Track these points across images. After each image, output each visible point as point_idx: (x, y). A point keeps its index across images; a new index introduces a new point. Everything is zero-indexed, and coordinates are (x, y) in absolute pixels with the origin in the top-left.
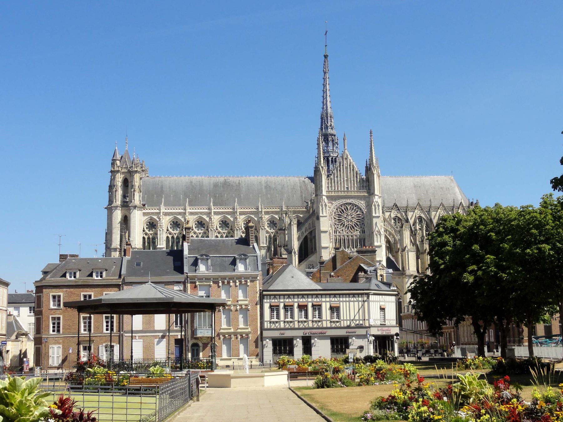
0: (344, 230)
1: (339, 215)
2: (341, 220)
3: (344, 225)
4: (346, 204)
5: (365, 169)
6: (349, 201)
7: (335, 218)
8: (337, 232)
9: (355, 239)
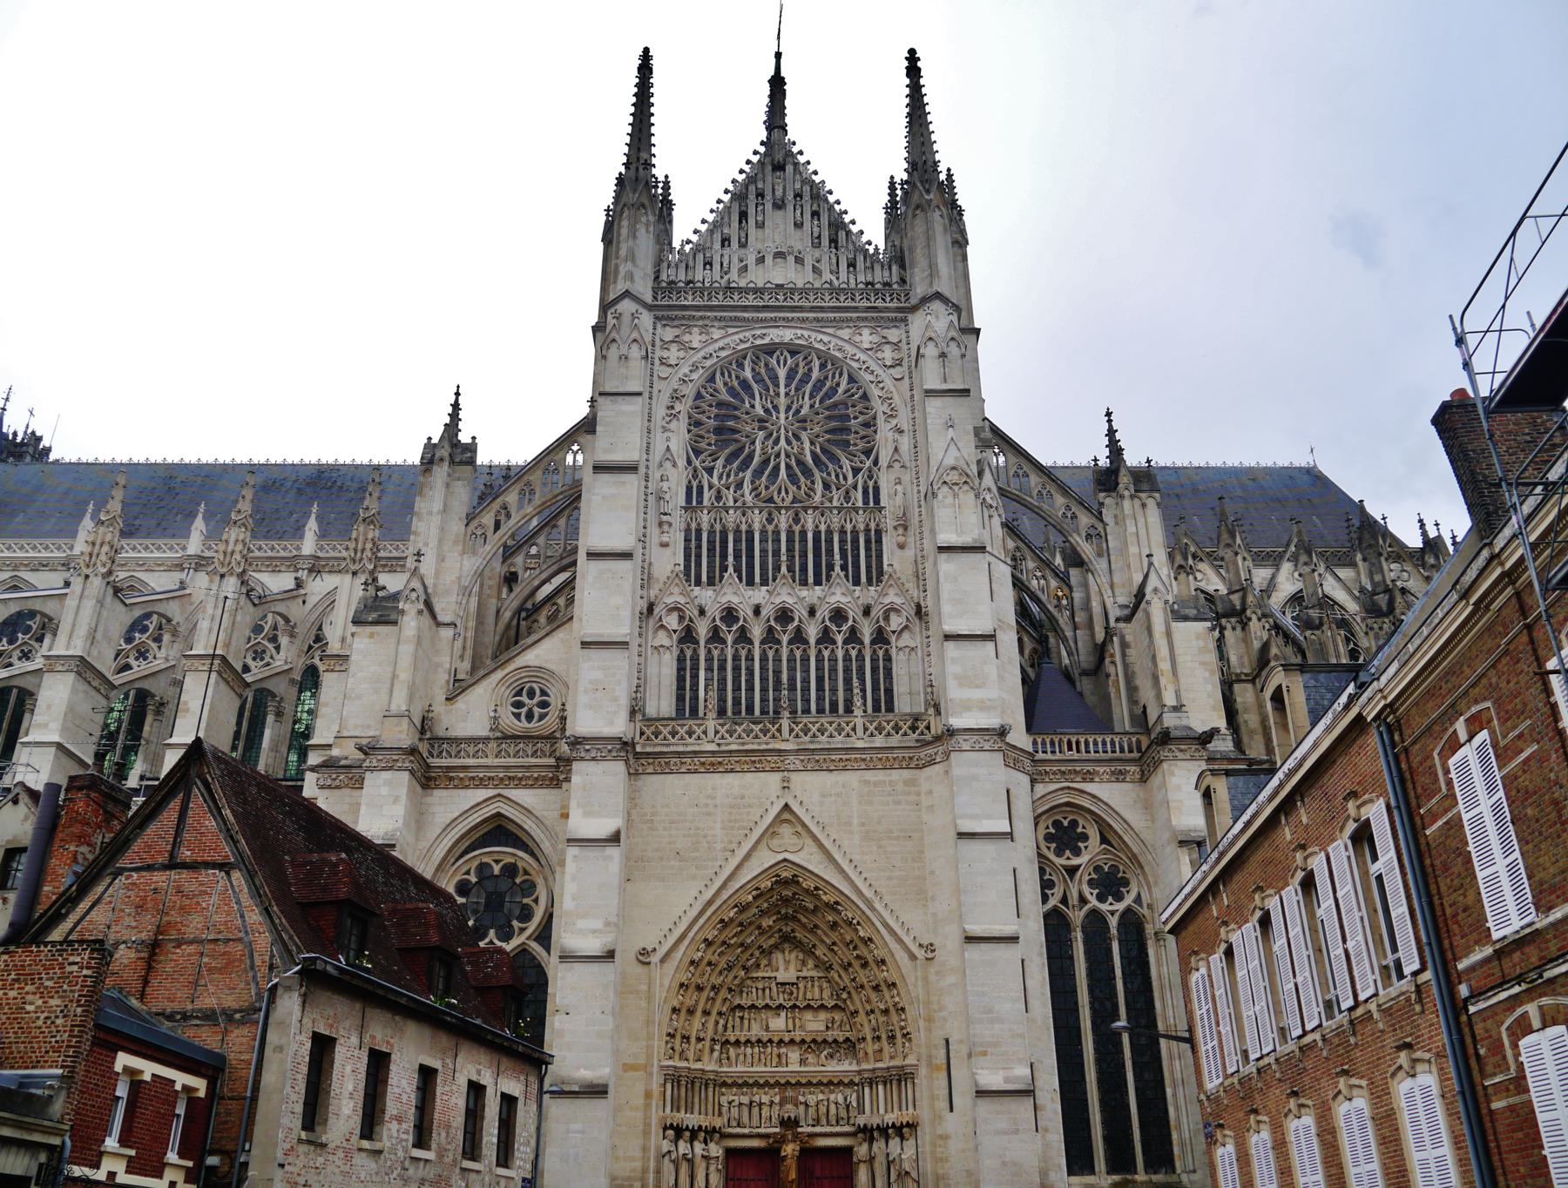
0: (747, 487)
1: (720, 404)
2: (735, 431)
3: (751, 456)
4: (770, 350)
6: (787, 335)
7: (698, 424)
9: (817, 534)
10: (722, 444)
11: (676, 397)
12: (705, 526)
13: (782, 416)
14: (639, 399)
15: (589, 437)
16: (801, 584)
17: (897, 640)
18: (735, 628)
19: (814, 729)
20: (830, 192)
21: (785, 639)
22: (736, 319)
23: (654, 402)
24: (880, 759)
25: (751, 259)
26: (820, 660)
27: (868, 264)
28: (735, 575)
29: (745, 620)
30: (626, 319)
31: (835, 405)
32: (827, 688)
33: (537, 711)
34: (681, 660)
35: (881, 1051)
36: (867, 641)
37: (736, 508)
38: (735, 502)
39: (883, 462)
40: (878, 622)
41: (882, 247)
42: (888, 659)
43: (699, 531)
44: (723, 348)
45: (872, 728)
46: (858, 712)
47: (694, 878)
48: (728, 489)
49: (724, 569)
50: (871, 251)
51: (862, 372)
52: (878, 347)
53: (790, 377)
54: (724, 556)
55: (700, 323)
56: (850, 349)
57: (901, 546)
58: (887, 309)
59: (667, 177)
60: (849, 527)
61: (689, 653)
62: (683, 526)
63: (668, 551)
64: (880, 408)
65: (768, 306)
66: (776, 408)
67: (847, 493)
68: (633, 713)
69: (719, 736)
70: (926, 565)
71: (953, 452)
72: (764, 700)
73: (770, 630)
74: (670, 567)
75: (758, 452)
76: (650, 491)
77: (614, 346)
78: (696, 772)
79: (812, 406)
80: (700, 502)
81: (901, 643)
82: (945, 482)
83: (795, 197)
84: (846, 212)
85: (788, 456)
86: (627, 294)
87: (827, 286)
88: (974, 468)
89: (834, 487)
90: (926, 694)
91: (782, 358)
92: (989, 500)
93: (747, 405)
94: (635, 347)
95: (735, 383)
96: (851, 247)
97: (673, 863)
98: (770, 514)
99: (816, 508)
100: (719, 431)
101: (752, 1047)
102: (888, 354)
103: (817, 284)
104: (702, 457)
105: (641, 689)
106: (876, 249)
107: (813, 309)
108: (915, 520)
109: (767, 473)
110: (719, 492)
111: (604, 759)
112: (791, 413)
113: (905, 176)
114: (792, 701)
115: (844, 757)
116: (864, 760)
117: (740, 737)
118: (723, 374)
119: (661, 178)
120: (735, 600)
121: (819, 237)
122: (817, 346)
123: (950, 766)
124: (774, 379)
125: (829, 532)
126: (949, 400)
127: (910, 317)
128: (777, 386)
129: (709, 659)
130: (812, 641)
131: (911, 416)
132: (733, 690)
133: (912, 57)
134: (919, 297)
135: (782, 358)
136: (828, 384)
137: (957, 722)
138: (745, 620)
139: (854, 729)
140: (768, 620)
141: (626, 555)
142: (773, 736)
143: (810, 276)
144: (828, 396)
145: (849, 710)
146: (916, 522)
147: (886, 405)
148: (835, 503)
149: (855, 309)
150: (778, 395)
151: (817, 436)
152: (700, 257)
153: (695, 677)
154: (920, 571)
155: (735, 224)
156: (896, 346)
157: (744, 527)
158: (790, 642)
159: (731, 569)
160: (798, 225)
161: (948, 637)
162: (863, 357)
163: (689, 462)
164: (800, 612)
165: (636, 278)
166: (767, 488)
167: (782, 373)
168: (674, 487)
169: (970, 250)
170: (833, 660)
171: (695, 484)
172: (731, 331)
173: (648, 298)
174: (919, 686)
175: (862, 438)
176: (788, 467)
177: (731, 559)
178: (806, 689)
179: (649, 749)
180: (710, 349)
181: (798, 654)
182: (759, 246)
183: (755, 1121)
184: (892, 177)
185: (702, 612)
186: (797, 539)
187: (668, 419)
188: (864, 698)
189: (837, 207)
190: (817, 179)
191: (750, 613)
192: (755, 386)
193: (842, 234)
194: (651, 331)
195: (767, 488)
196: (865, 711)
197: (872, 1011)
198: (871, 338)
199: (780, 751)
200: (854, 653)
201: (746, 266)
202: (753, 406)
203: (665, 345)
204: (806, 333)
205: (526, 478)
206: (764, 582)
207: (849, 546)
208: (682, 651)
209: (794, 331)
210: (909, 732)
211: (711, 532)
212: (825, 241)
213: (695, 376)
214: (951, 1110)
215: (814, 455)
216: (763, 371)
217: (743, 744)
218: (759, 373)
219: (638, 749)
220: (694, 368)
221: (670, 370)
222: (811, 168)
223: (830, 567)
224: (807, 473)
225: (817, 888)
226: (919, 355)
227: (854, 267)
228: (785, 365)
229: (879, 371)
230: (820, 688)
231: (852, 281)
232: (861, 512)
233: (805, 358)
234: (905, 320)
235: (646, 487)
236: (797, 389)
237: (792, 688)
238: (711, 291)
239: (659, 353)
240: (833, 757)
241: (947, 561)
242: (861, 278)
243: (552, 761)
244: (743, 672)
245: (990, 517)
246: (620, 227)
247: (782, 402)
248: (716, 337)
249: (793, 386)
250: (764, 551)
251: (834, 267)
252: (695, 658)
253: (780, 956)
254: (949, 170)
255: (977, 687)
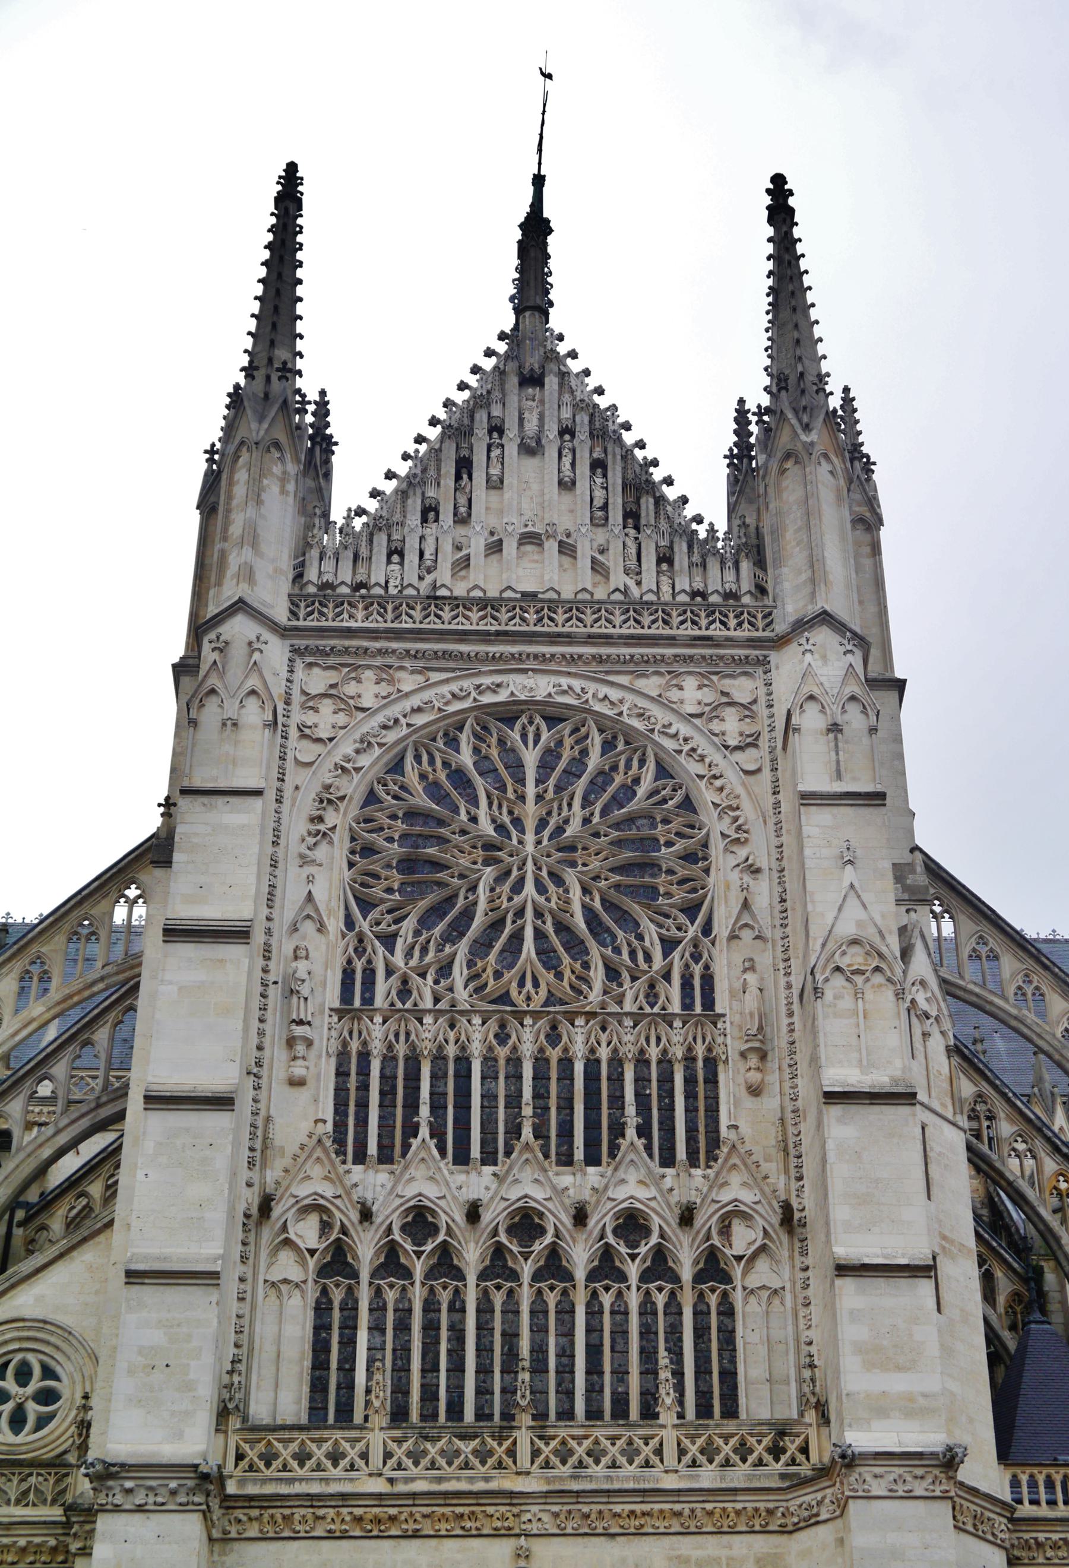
0: (459, 973)
1: (412, 815)
2: (438, 865)
3: (468, 914)
5: (722, 471)
7: (368, 851)
8: (381, 986)
9: (592, 1065)
10: (413, 890)
11: (328, 799)
12: (377, 1048)
13: (530, 838)
14: (257, 803)
15: (159, 873)
16: (559, 1163)
17: (745, 1273)
18: (429, 1247)
19: (580, 1451)
20: (627, 426)
21: (527, 1270)
22: (447, 655)
23: (285, 808)
24: (710, 1514)
25: (477, 546)
26: (594, 1311)
27: (696, 558)
28: (432, 1144)
29: (449, 1232)
30: (238, 652)
31: (631, 820)
32: (607, 1368)
33: (33, 1409)
34: (322, 1308)
36: (687, 1274)
37: (438, 1014)
38: (437, 1000)
39: (721, 928)
40: (708, 1237)
41: (722, 527)
42: (727, 1311)
43: (364, 1057)
44: (419, 710)
45: (693, 1449)
46: (667, 1417)
48: (423, 975)
49: (411, 1130)
50: (702, 534)
51: (682, 759)
52: (711, 713)
53: (545, 766)
54: (412, 1105)
55: (378, 661)
56: (660, 715)
57: (755, 1091)
58: (730, 642)
59: (323, 393)
60: (654, 1053)
61: (337, 1296)
62: (334, 1046)
63: (303, 1095)
64: (714, 824)
65: (506, 633)
66: (517, 822)
67: (652, 986)
68: (223, 1414)
69: (390, 1463)
70: (802, 1127)
71: (853, 911)
72: (483, 1391)
73: (499, 1251)
74: (307, 1126)
75: (482, 906)
76: (272, 977)
77: (213, 700)
78: (344, 1536)
79: (586, 821)
80: (368, 999)
81: (754, 1280)
82: (838, 969)
83: (562, 432)
84: (655, 463)
85: (539, 914)
86: (240, 606)
87: (617, 596)
88: (894, 944)
89: (626, 975)
90: (801, 1381)
91: (531, 730)
92: (922, 1004)
93: (463, 817)
94: (252, 703)
95: (442, 776)
96: (664, 525)
98: (503, 1026)
99: (591, 1015)
100: (407, 865)
102: (732, 725)
103: (600, 594)
104: (374, 914)
105: (242, 1367)
106: (712, 530)
107: (591, 639)
108: (781, 1041)
109: (498, 946)
110: (405, 981)
111: (160, 1508)
112: (546, 833)
113: (765, 401)
114: (539, 1393)
115: (638, 1508)
116: (678, 1514)
117: (433, 1465)
118: (418, 758)
119: (313, 396)
120: (431, 1191)
121: (605, 507)
122: (598, 707)
123: (847, 1529)
124: (517, 768)
125: (616, 1062)
126: (845, 813)
127: (774, 657)
128: (522, 781)
129: (378, 1308)
130: (580, 1274)
131: (775, 842)
132: (423, 1371)
133: (779, 188)
134: (791, 619)
135: (531, 730)
136: (618, 779)
137: (859, 1439)
138: (449, 1232)
139: (659, 1452)
140: (495, 1233)
141: (222, 1102)
142: (500, 1465)
143: (587, 578)
144: (617, 801)
145: (649, 1413)
146: (784, 1044)
147: (727, 820)
148: (629, 1006)
149: (671, 641)
150: (522, 798)
151: (596, 878)
152: (381, 540)
153: (349, 1343)
154: (791, 1140)
155: (449, 482)
156: (748, 710)
157: (451, 1051)
158: (537, 1277)
159: (424, 1132)
160: (566, 485)
161: (843, 1269)
162: (684, 730)
163: (350, 923)
164: (557, 1217)
165: (259, 576)
166: (498, 975)
167: (531, 758)
168: (317, 968)
169: (886, 535)
170: (620, 1312)
171: (359, 965)
172: (435, 676)
173: (281, 614)
174: (788, 1366)
175: (682, 882)
176: (540, 935)
177: (425, 1111)
178: (566, 1370)
179: (252, 1490)
180: (395, 711)
181: (552, 1299)
182: (493, 522)
184: (741, 402)
185: (366, 1215)
186: (554, 1075)
187: (311, 840)
188: (680, 1388)
189: (639, 454)
190: (603, 402)
191: (460, 1217)
192: (479, 782)
193: (647, 504)
194: (284, 674)
195: (498, 975)
196: (681, 1416)
198: (699, 695)
199: (511, 1494)
200: (660, 1299)
201: (468, 558)
202: (474, 819)
203: (310, 703)
204: (577, 684)
205: (34, 949)
206: (489, 1157)
207: (654, 1089)
208: (325, 1291)
209: (554, 679)
210: (768, 1458)
211: (389, 1059)
212: (616, 515)
213: (364, 761)
215: (591, 917)
216: (494, 752)
217: (439, 1480)
218: (487, 757)
219: (231, 1488)
220: (365, 745)
221: (318, 748)
222: (592, 382)
223: (618, 1130)
224: (576, 946)
226: (788, 726)
227: (670, 561)
228: (536, 742)
229: (715, 756)
230: (594, 1368)
231: (666, 588)
232: (677, 1024)
233: (576, 730)
234: (763, 662)
235: (265, 971)
236: (559, 789)
237: (539, 1367)
238: (400, 604)
239: (298, 716)
240: (617, 1509)
241: (840, 1120)
242: (683, 583)
243: (56, 1513)
244: (444, 1334)
245: (926, 1035)
246: (231, 483)
247: (531, 811)
248: (406, 688)
249: (552, 782)
250: (488, 1098)
251: (632, 563)
252: (350, 1307)
254: (846, 390)
255: (899, 1368)
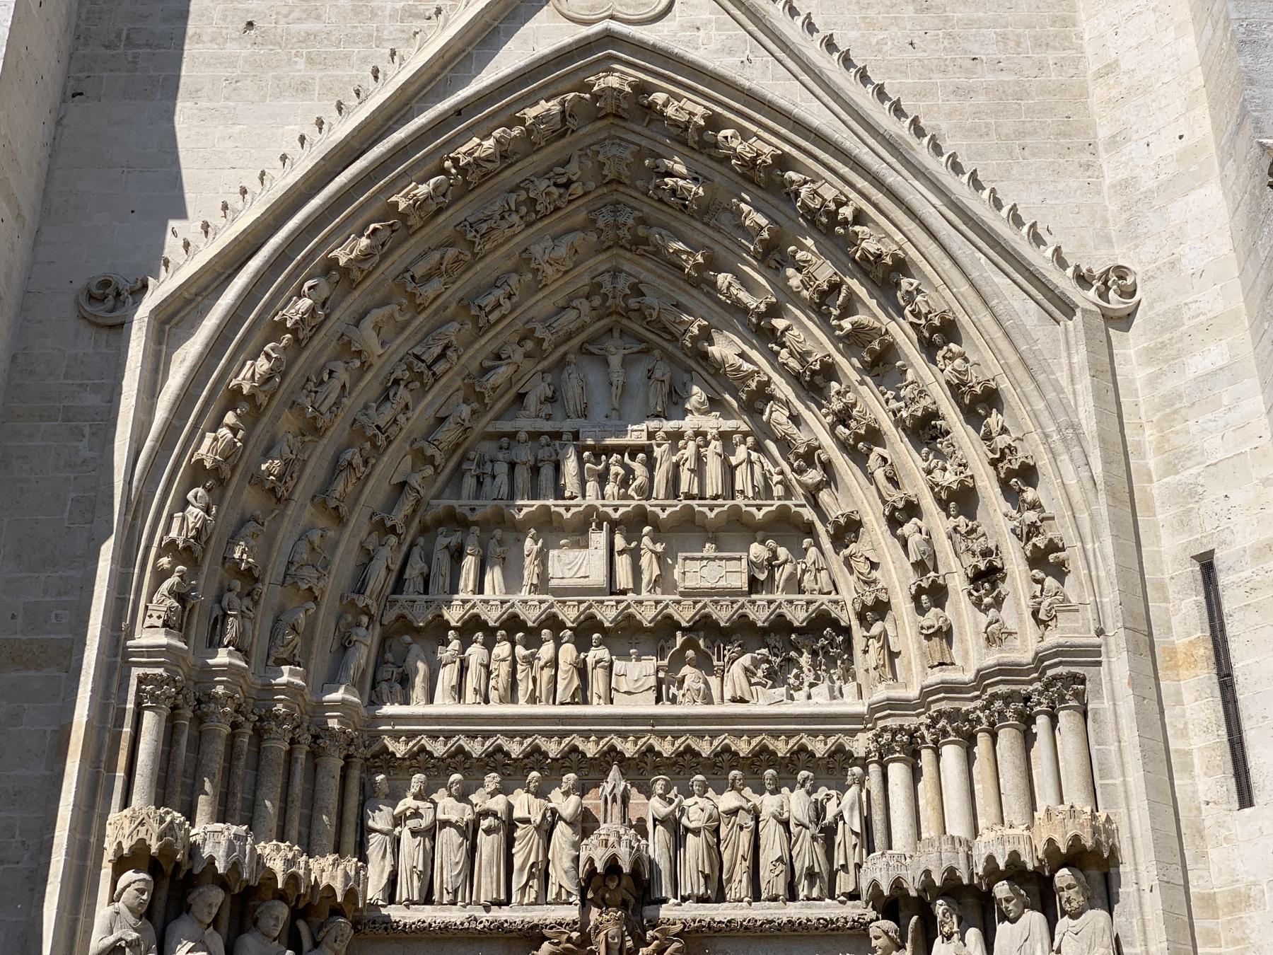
35: (945, 634)
47: (303, 88)
97: (232, 48)
101: (489, 645)
183: (487, 885)
197: (913, 509)
214: (1245, 797)
225: (714, 122)
253: (594, 376)
